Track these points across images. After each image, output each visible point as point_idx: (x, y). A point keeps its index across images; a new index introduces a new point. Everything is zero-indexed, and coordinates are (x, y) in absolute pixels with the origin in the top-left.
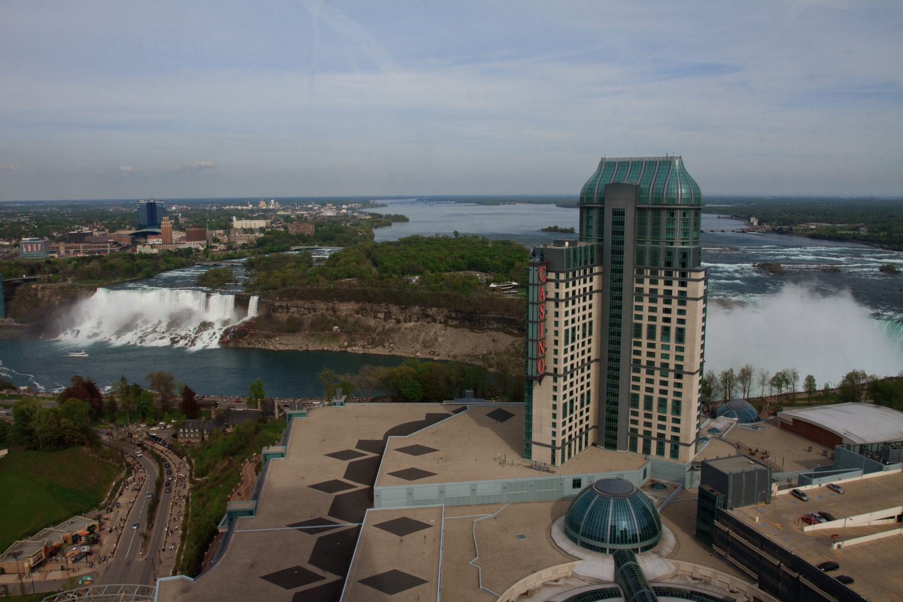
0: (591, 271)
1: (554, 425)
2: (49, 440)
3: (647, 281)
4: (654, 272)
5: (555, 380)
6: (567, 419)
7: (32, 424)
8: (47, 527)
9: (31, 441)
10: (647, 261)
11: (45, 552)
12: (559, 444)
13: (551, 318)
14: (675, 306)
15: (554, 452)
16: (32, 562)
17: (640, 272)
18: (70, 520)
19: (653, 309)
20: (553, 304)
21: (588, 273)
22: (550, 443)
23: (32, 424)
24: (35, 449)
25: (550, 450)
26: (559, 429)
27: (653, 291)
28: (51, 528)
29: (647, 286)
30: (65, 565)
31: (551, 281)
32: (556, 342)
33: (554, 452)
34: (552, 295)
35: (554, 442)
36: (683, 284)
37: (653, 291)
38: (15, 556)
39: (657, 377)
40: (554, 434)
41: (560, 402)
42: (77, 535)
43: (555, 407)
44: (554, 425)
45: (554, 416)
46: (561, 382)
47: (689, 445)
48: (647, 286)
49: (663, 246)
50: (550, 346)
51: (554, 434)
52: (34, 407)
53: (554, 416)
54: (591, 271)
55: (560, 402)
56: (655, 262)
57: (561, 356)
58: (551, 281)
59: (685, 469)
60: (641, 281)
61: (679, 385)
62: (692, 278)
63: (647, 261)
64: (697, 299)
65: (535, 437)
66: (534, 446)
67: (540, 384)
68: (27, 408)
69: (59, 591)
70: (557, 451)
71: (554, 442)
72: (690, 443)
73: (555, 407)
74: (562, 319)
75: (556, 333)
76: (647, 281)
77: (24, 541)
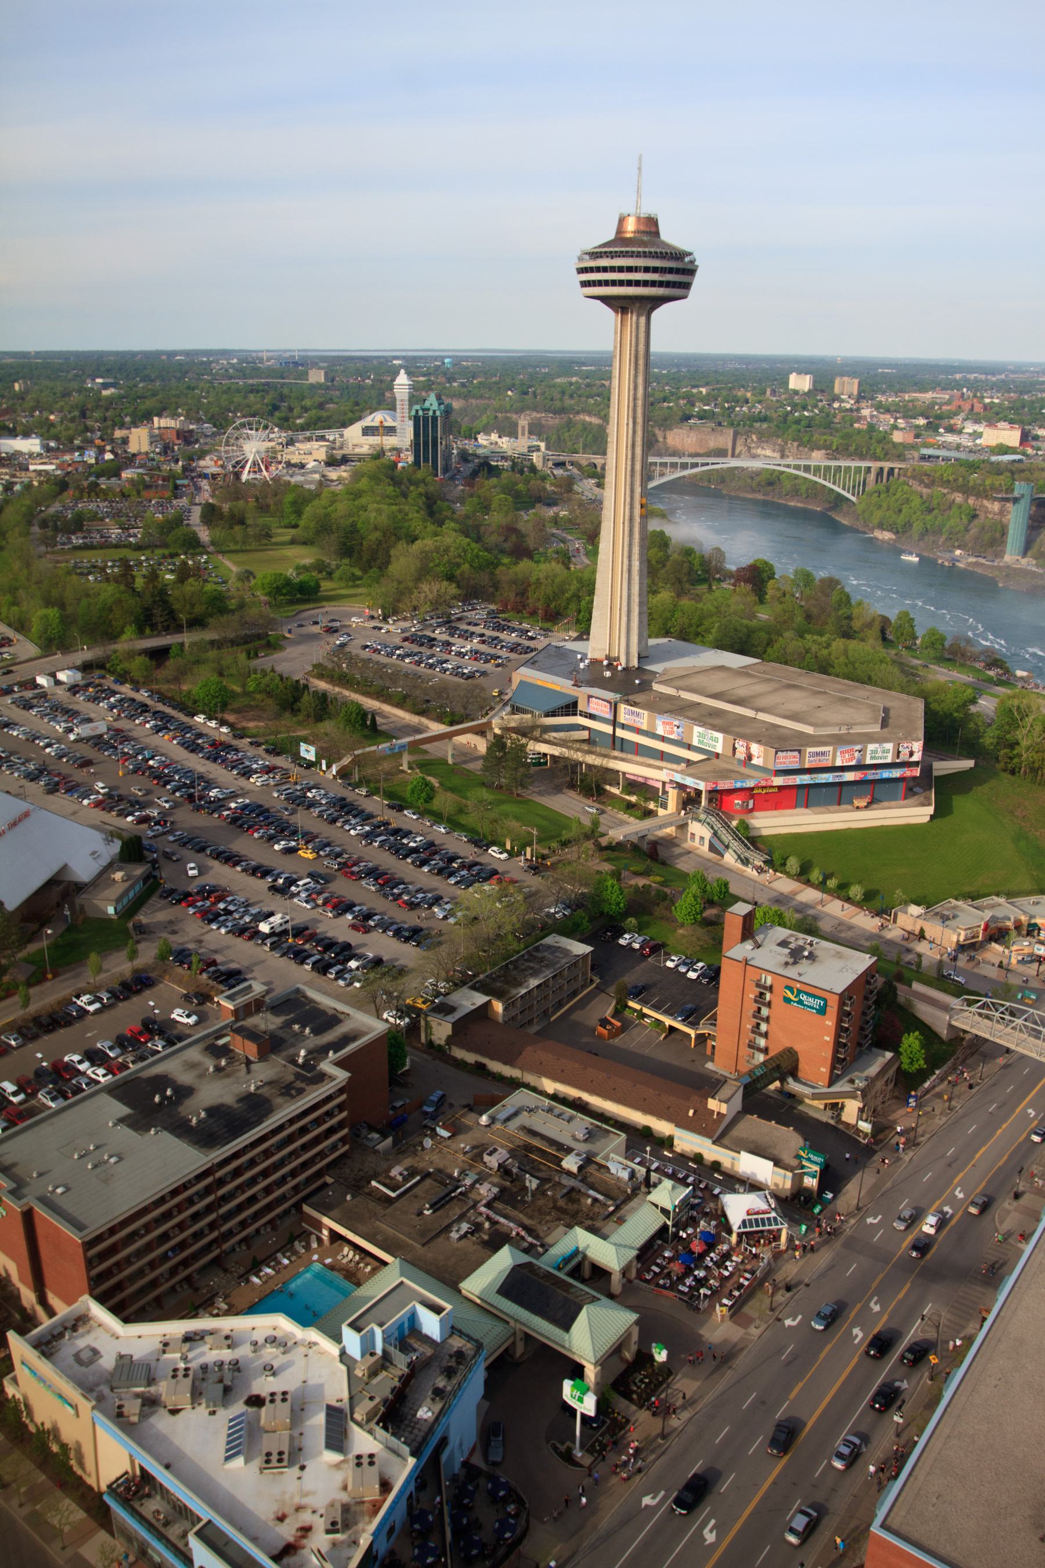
2: (1036, 765)
7: (1019, 734)
8: (997, 895)
9: (1011, 758)
11: (985, 929)
16: (962, 938)
18: (1033, 899)
23: (1019, 734)
24: (1013, 772)
28: (1001, 900)
30: (1005, 961)
38: (945, 919)
42: (1035, 925)
52: (1029, 707)
68: (1018, 708)
69: (986, 996)
77: (960, 903)
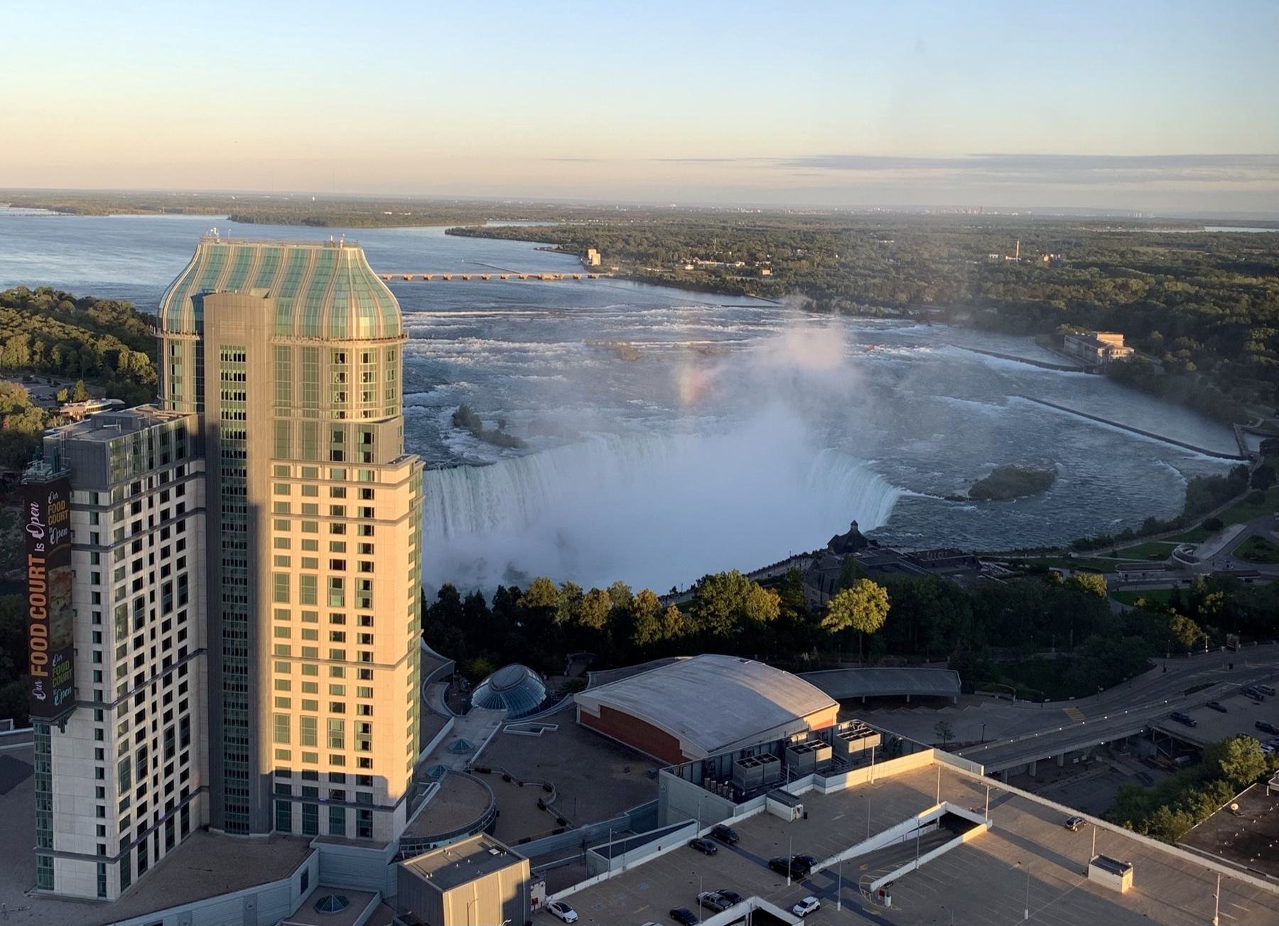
0: (180, 472)
1: (101, 812)
3: (296, 488)
4: (310, 474)
5: (100, 717)
6: (133, 792)
10: (296, 450)
12: (113, 850)
13: (84, 589)
14: (353, 537)
15: (102, 868)
17: (283, 472)
19: (310, 545)
20: (87, 556)
21: (171, 480)
22: (94, 852)
25: (93, 866)
26: (113, 820)
27: (310, 510)
29: (296, 499)
31: (82, 507)
32: (98, 637)
33: (102, 868)
34: (83, 537)
35: (102, 848)
36: (367, 494)
37: (310, 510)
39: (324, 677)
40: (102, 831)
41: (113, 761)
43: (101, 773)
44: (101, 812)
45: (101, 792)
46: (113, 720)
47: (392, 809)
48: (296, 499)
49: (327, 418)
50: (86, 648)
51: (102, 831)
53: (101, 792)
54: (180, 472)
55: (113, 761)
56: (309, 452)
57: (112, 664)
58: (82, 507)
59: (385, 860)
60: (284, 490)
61: (369, 693)
62: (382, 482)
63: (296, 450)
64: (394, 522)
65: (60, 841)
66: (57, 862)
67: (63, 731)
70: (108, 866)
71: (102, 848)
72: (394, 804)
73: (101, 773)
74: (110, 589)
75: (98, 618)
76: (296, 488)
